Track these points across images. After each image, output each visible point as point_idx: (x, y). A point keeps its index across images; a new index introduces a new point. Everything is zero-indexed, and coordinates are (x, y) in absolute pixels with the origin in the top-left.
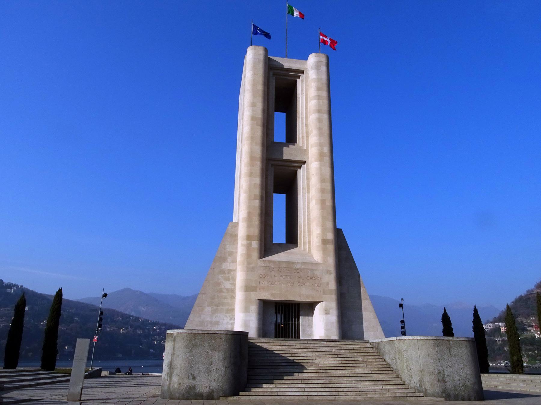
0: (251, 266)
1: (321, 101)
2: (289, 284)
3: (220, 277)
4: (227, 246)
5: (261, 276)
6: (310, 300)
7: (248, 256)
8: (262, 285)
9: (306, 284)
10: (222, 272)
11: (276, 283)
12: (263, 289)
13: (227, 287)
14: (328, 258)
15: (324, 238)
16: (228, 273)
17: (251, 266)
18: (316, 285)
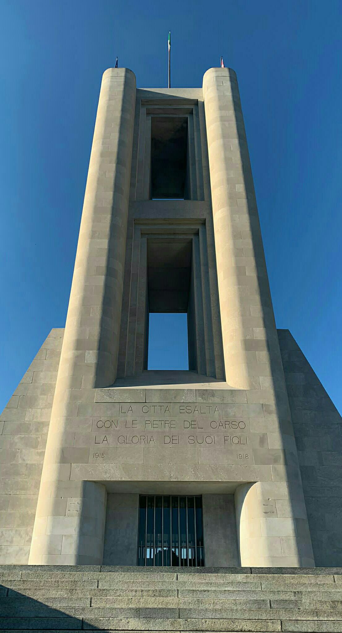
0: (79, 402)
1: (227, 124)
2: (167, 440)
3: (16, 439)
4: (42, 375)
5: (100, 424)
6: (222, 477)
7: (75, 381)
8: (101, 446)
9: (209, 440)
10: (23, 428)
11: (135, 440)
12: (103, 455)
13: (29, 462)
14: (261, 378)
15: (248, 337)
16: (37, 430)
17: (79, 402)
18: (236, 440)
